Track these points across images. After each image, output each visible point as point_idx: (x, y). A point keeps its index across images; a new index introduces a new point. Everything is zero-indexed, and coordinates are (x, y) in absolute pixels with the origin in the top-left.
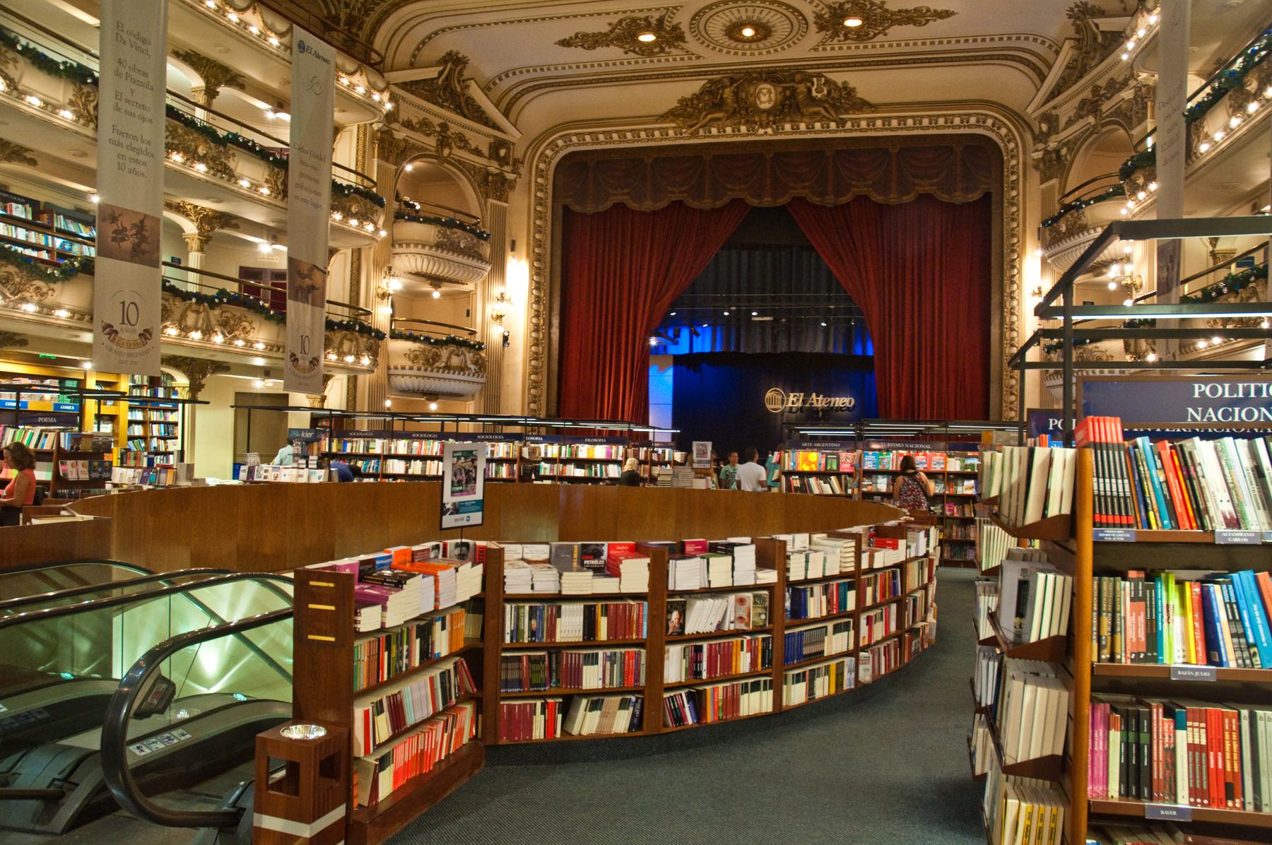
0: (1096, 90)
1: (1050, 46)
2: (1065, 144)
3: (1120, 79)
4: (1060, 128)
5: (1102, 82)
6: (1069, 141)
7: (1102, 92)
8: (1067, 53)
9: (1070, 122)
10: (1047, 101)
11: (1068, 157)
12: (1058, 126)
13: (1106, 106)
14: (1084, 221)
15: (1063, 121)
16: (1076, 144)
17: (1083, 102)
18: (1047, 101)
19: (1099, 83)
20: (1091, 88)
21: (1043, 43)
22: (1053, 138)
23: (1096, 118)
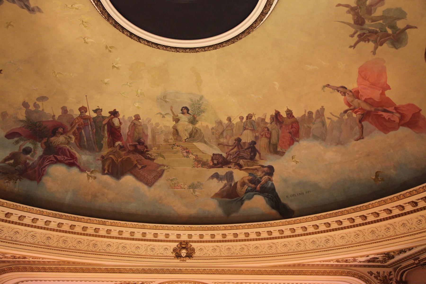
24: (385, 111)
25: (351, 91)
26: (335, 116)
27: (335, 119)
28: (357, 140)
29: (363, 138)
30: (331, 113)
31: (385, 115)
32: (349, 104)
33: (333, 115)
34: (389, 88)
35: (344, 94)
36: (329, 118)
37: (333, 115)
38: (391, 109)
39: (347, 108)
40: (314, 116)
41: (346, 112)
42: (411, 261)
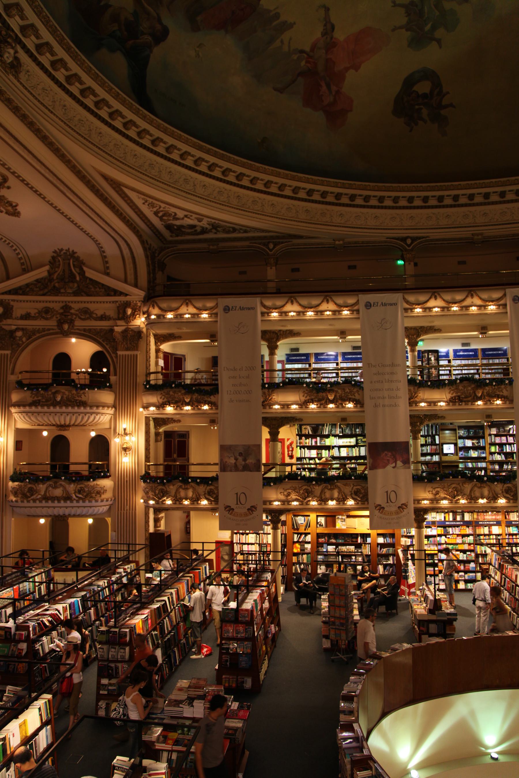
0: (66, 308)
1: (20, 259)
2: (23, 329)
3: (100, 313)
4: (14, 316)
5: (76, 307)
6: (26, 328)
7: (72, 311)
8: (42, 273)
9: (27, 317)
10: (9, 292)
11: (24, 339)
12: (12, 314)
13: (78, 323)
14: (84, 398)
15: (18, 312)
16: (34, 334)
17: (47, 310)
18: (9, 292)
19: (72, 305)
20: (64, 304)
21: (18, 254)
22: (9, 321)
23: (69, 328)
24: (328, 86)
25: (332, 38)
26: (289, 47)
27: (286, 48)
28: (275, 89)
29: (281, 93)
30: (291, 39)
31: (324, 88)
32: (314, 47)
33: (289, 43)
34: (357, 68)
35: (324, 34)
36: (282, 42)
37: (289, 43)
38: (334, 88)
39: (307, 49)
40: (275, 23)
41: (302, 52)
42: (204, 245)
